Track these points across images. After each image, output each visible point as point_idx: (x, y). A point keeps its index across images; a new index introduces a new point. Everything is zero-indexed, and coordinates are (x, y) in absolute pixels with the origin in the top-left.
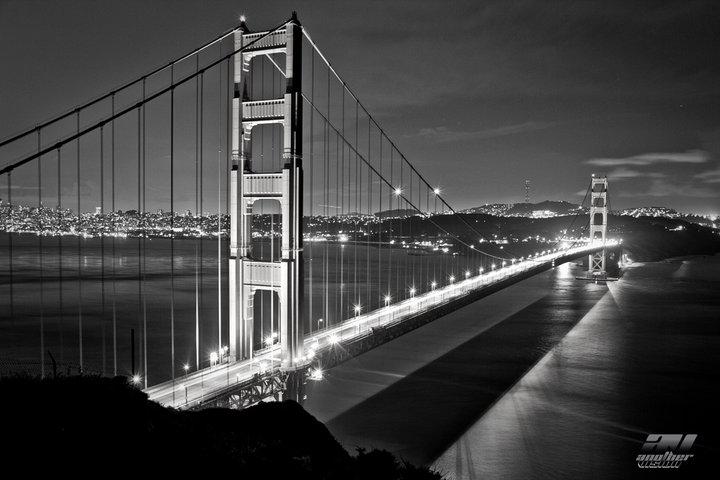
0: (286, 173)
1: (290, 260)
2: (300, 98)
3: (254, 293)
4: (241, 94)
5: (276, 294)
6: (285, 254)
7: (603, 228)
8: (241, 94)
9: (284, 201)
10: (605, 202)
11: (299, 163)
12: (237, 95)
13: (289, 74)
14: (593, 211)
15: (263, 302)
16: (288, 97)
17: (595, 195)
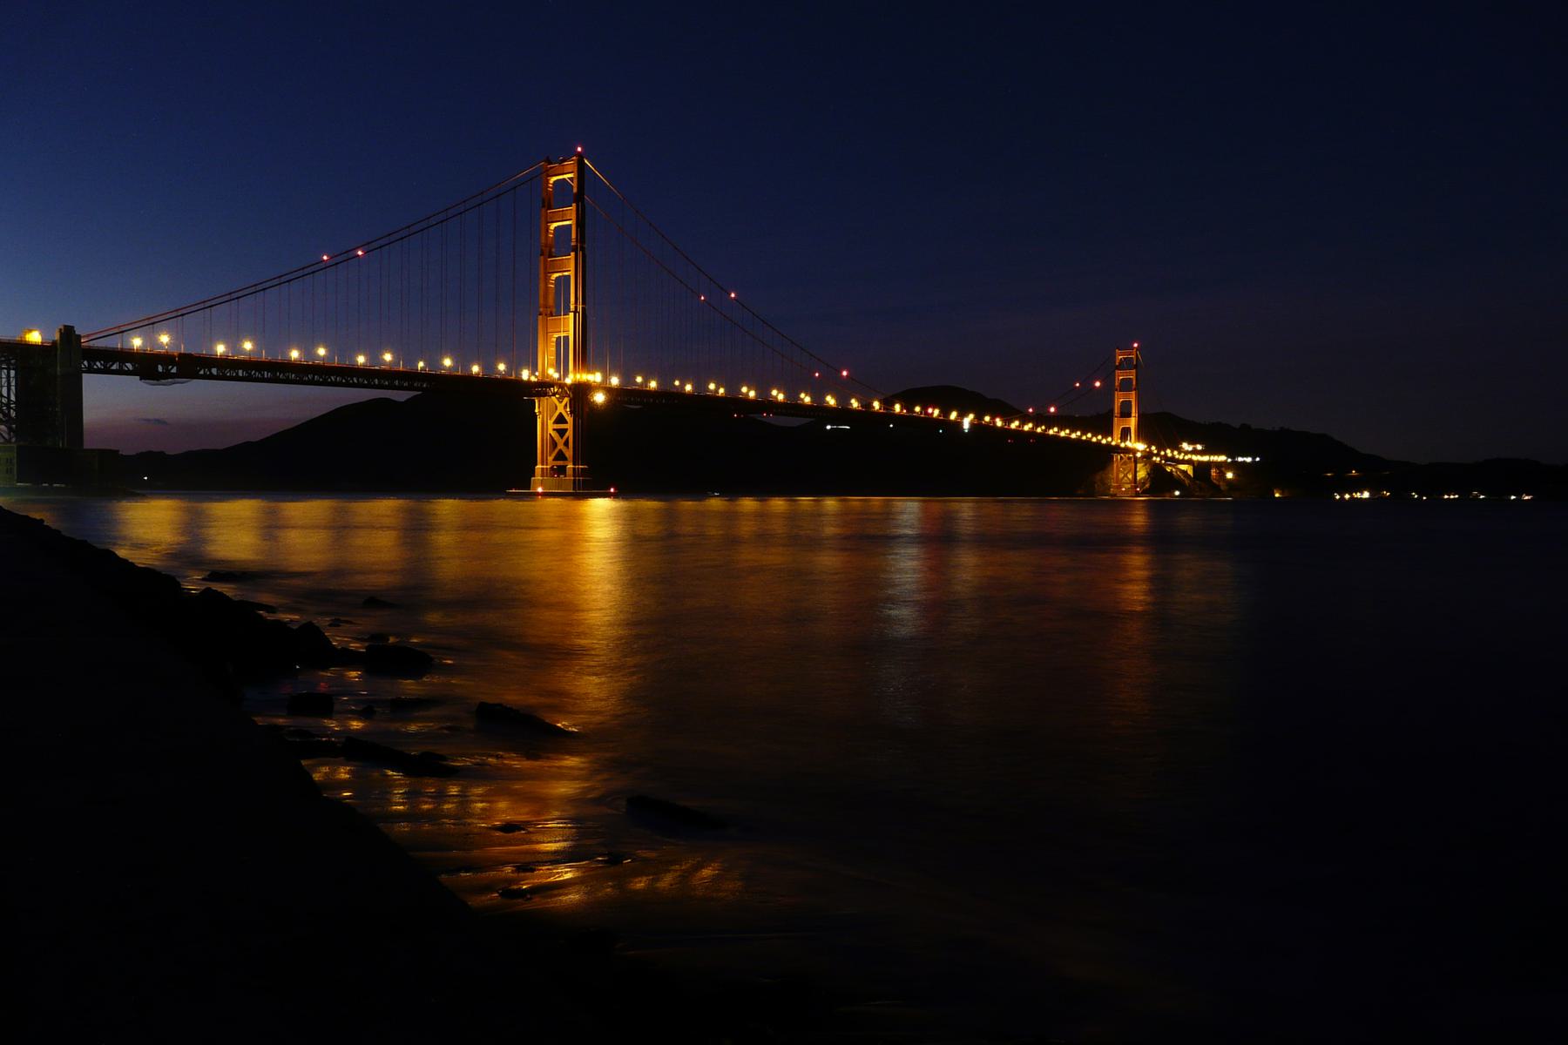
0: (573, 254)
1: (575, 312)
2: (583, 207)
3: (555, 340)
4: (546, 204)
5: (566, 338)
6: (572, 307)
7: (1132, 423)
8: (546, 204)
9: (572, 273)
10: (1134, 383)
11: (583, 249)
12: (543, 206)
13: (575, 190)
14: (1119, 398)
15: (562, 344)
16: (574, 205)
17: (1120, 376)
